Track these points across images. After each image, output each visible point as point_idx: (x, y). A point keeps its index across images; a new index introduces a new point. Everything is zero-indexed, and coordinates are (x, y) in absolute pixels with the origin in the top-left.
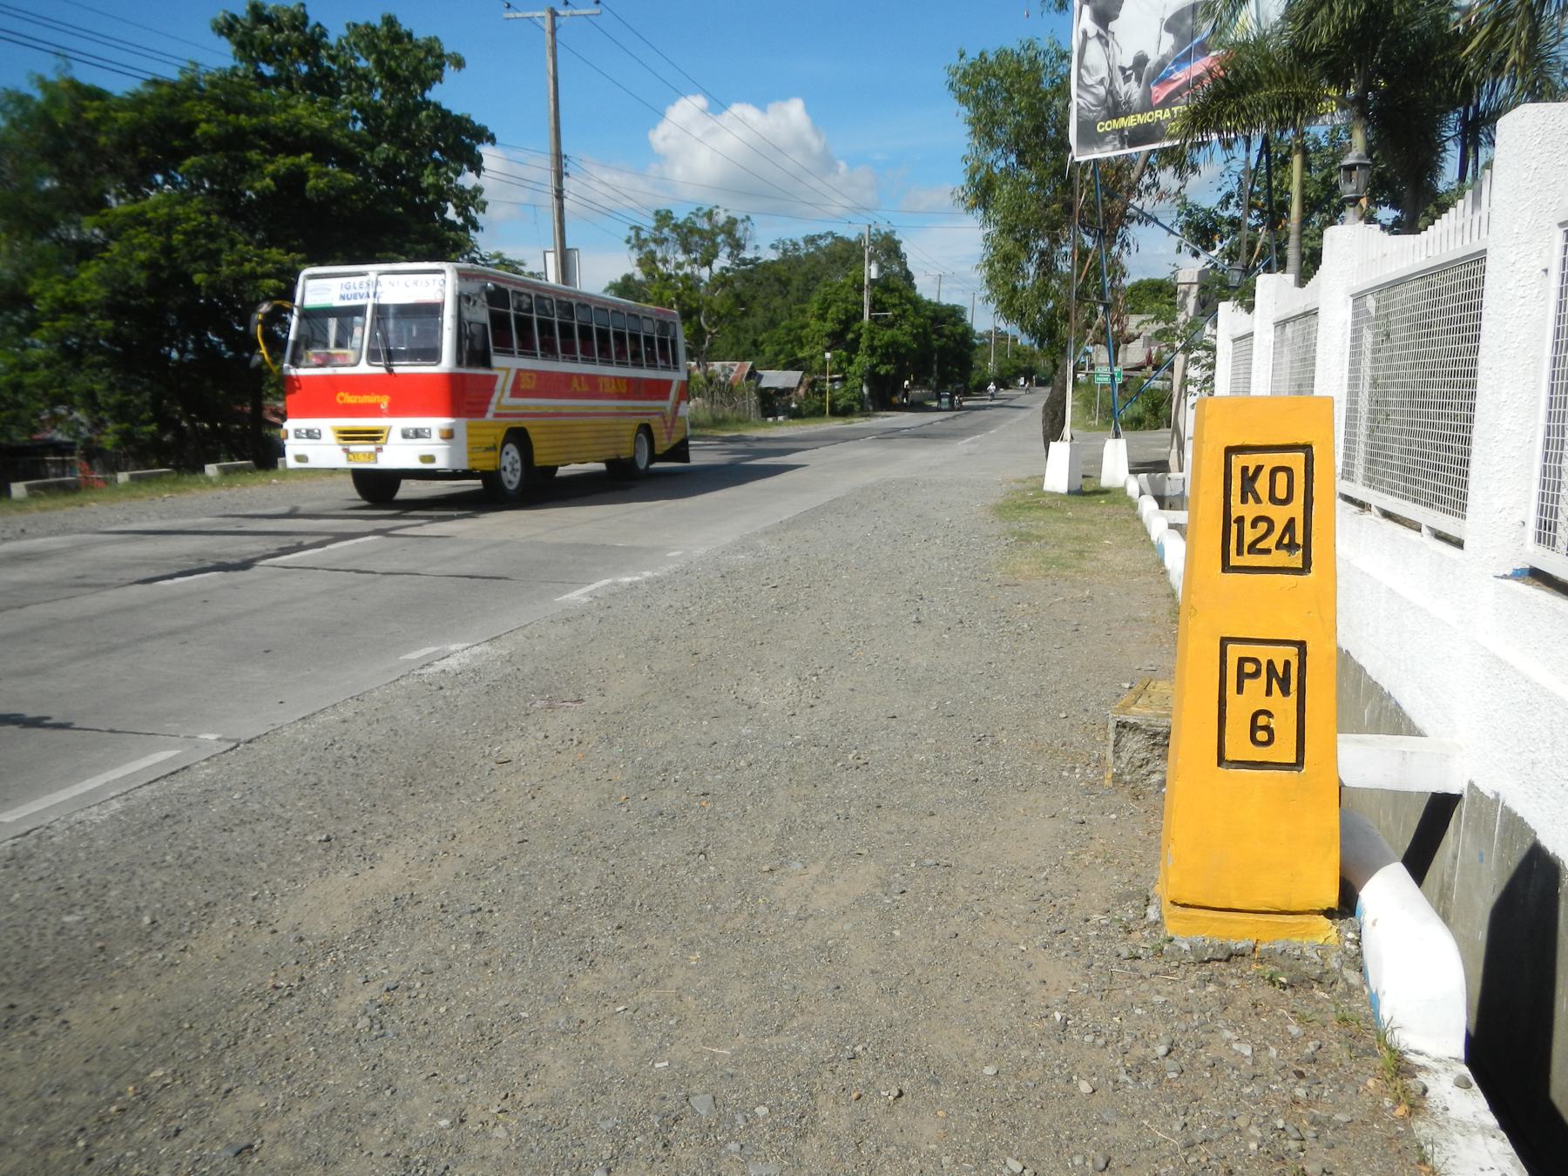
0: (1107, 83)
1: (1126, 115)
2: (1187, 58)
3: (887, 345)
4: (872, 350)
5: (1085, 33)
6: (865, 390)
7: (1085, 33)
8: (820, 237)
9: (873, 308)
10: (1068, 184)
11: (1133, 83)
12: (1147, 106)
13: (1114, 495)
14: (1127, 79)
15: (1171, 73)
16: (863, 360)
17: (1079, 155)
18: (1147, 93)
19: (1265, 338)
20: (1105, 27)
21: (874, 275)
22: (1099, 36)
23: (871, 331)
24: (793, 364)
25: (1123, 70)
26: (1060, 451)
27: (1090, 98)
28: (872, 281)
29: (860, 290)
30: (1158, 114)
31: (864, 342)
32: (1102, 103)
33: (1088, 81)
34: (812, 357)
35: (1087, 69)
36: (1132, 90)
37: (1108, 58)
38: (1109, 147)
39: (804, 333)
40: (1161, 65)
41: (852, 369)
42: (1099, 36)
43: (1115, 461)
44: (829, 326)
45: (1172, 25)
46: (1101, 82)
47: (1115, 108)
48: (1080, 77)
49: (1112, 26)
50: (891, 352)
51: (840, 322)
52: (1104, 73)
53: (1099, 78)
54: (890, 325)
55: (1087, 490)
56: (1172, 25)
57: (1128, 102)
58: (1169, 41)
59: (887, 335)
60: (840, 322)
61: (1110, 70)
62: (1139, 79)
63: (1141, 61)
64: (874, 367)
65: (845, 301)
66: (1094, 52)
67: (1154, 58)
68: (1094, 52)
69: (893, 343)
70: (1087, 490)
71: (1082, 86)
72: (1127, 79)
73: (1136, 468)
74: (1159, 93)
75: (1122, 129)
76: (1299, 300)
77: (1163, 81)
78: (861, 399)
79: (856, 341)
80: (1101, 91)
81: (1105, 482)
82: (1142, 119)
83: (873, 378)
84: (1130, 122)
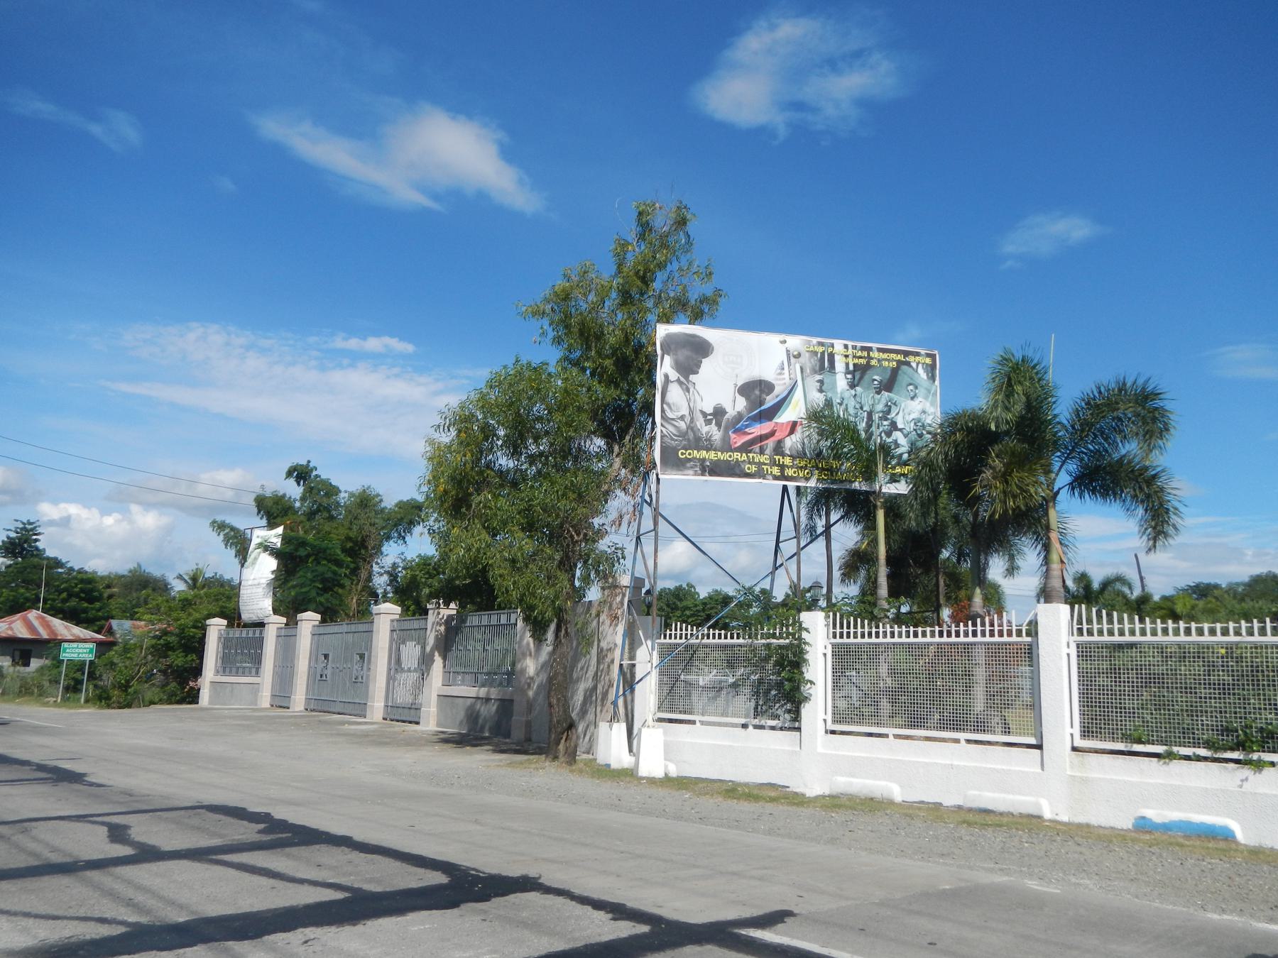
0: (688, 419)
1: (708, 450)
5: (666, 376)
7: (666, 376)
11: (713, 427)
14: (708, 422)
15: (747, 426)
18: (726, 439)
20: (687, 378)
22: (678, 381)
25: (704, 414)
27: (671, 429)
30: (737, 455)
32: (683, 435)
33: (670, 415)
35: (669, 405)
36: (716, 434)
37: (689, 401)
38: (691, 472)
40: (739, 416)
42: (678, 381)
46: (682, 418)
47: (699, 442)
48: (663, 411)
49: (692, 377)
52: (685, 411)
53: (680, 414)
57: (709, 440)
58: (741, 404)
61: (691, 411)
62: (719, 425)
63: (719, 412)
67: (731, 413)
68: (675, 393)
71: (664, 417)
72: (708, 422)
74: (740, 441)
75: (704, 460)
77: (739, 431)
80: (682, 425)
82: (721, 456)
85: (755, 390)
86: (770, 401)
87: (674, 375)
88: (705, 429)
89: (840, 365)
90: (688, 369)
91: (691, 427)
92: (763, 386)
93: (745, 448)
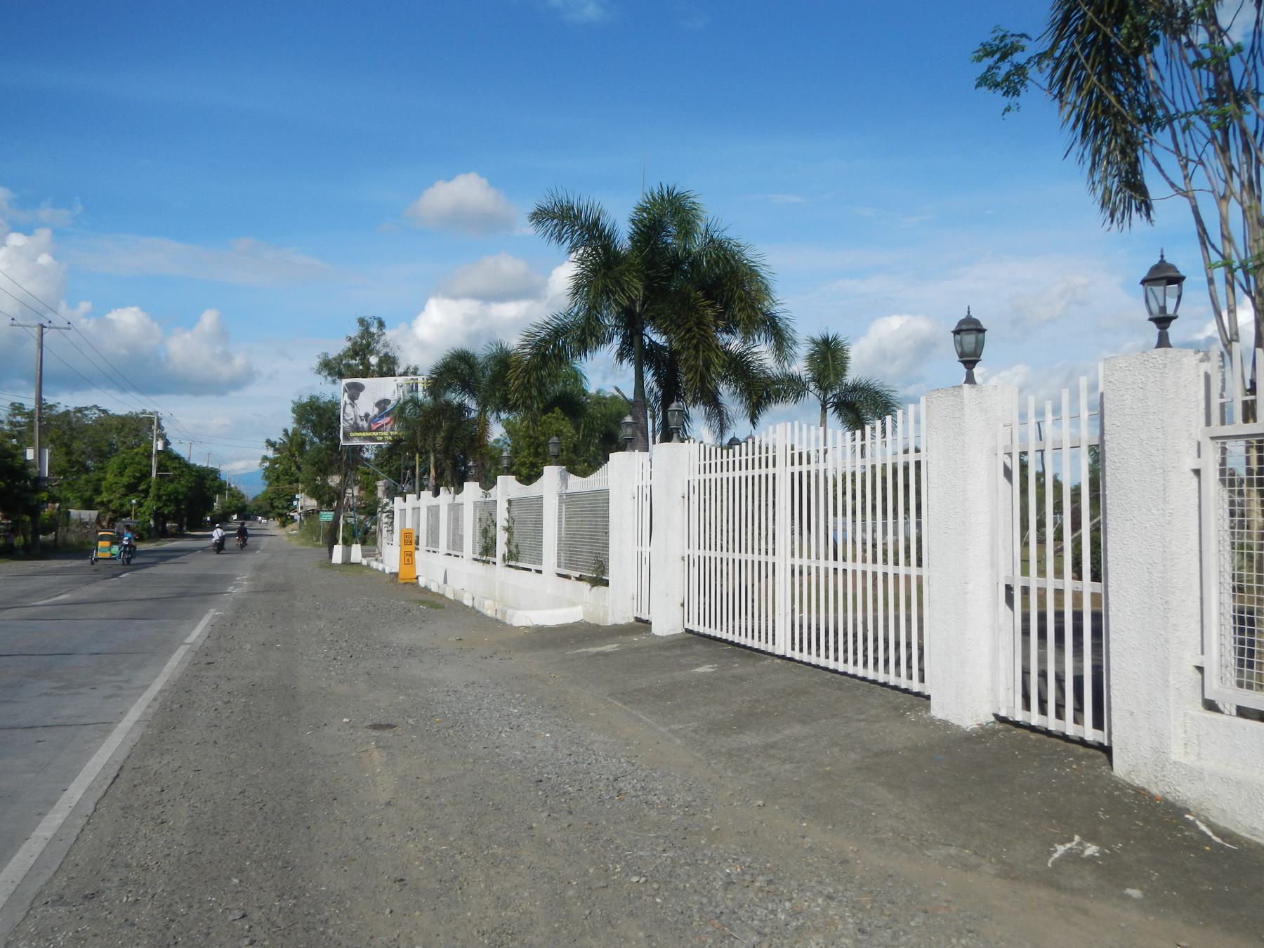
2: (382, 417)
3: (169, 495)
4: (159, 497)
6: (152, 522)
8: (86, 408)
9: (158, 470)
10: (340, 453)
12: (370, 430)
13: (359, 564)
16: (151, 503)
17: (342, 443)
19: (409, 512)
21: (160, 447)
23: (158, 484)
24: (88, 505)
26: (338, 550)
28: (158, 452)
29: (149, 456)
31: (153, 492)
34: (110, 501)
36: (365, 424)
39: (104, 483)
41: (142, 510)
43: (356, 551)
44: (125, 480)
45: (378, 404)
47: (357, 428)
50: (174, 498)
51: (134, 477)
54: (171, 481)
55: (347, 562)
56: (378, 404)
58: (376, 410)
59: (171, 487)
60: (134, 477)
63: (367, 415)
64: (158, 508)
65: (139, 463)
66: (349, 408)
67: (372, 415)
68: (349, 408)
69: (176, 492)
70: (347, 562)
73: (364, 556)
76: (416, 504)
77: (376, 423)
78: (149, 530)
79: (146, 492)
81: (353, 560)
83: (157, 515)
84: (364, 434)
85: (382, 404)
86: (389, 408)
87: (348, 401)
88: (360, 423)
89: (420, 388)
90: (353, 398)
91: (355, 423)
92: (386, 402)
93: (377, 430)
